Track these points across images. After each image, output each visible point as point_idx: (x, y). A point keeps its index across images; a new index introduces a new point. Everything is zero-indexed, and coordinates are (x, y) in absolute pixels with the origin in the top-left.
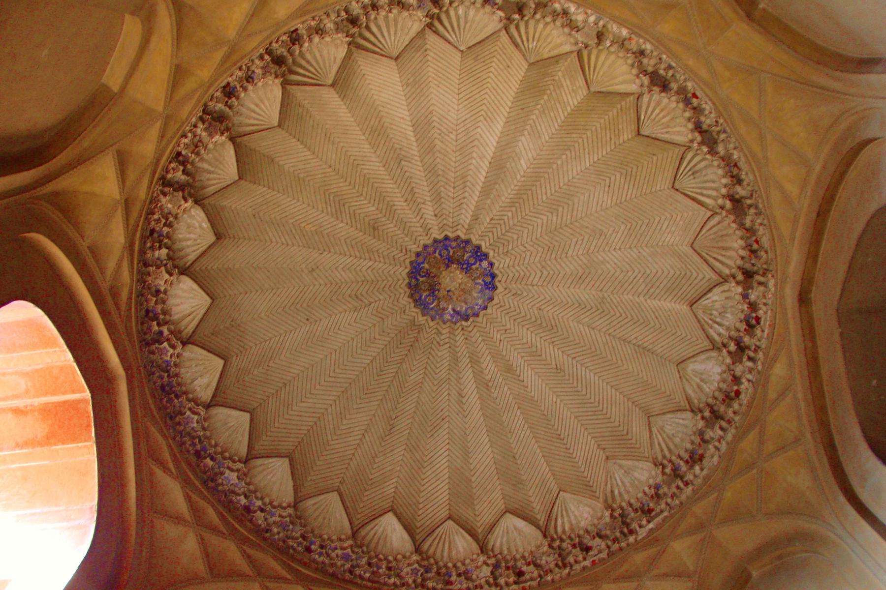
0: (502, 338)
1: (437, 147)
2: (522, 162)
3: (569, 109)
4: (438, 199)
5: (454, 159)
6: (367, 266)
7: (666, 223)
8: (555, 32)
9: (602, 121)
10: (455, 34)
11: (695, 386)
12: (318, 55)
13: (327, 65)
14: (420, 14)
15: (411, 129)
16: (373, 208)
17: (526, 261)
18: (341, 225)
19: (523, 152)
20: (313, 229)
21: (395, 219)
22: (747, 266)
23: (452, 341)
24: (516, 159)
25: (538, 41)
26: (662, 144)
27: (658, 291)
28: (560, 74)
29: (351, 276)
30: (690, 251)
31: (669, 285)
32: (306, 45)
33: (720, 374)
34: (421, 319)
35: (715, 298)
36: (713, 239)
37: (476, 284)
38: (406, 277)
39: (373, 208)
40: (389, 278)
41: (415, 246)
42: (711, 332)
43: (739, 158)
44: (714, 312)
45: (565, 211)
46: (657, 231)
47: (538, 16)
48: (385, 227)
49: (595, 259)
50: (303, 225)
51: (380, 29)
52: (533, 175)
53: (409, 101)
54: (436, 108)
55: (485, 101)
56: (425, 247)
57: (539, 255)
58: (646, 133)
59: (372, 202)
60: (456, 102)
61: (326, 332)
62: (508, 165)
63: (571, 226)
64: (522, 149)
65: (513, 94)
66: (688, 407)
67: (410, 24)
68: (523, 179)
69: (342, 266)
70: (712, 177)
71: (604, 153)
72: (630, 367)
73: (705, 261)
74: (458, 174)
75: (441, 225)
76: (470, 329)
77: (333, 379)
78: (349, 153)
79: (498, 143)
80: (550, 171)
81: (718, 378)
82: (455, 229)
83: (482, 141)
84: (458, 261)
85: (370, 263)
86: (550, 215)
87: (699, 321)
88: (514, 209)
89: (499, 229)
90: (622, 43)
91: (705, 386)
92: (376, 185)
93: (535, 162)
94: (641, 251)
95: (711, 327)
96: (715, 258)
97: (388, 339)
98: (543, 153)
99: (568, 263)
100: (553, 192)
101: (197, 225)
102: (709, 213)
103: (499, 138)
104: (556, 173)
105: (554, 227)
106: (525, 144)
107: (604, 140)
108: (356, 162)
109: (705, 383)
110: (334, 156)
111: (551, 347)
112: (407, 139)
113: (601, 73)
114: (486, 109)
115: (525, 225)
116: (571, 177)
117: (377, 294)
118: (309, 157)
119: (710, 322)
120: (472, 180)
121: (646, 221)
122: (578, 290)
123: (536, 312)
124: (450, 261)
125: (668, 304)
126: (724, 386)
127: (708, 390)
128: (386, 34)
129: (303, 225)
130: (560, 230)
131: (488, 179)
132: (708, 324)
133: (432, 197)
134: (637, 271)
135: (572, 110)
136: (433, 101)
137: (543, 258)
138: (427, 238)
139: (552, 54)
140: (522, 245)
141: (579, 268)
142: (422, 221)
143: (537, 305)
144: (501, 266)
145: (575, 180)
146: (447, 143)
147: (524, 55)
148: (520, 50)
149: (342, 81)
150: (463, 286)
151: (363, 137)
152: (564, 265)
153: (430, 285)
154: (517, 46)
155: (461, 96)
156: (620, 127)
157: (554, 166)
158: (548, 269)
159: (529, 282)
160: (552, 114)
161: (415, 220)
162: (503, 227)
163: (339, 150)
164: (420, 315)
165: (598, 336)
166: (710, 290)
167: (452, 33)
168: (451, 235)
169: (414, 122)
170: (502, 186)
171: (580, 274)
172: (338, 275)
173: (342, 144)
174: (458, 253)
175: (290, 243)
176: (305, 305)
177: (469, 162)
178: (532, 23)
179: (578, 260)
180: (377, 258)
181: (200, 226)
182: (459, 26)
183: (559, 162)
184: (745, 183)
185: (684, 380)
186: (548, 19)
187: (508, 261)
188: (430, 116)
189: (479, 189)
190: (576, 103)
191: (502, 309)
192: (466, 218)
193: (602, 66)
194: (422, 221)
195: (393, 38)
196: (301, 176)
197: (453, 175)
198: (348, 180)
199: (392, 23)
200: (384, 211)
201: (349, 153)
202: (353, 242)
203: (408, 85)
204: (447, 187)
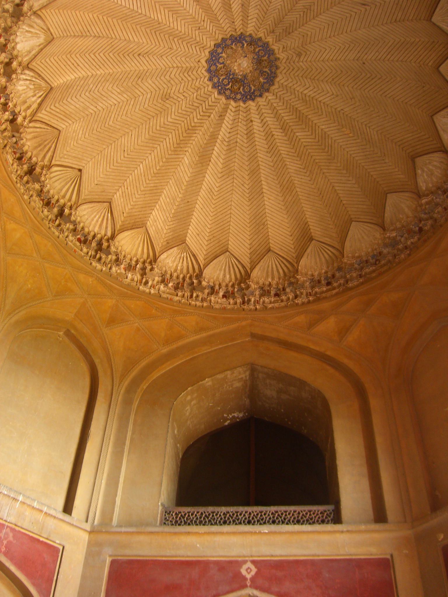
0: (202, 23)
1: (247, 173)
2: (187, 162)
3: (158, 207)
4: (250, 134)
5: (236, 164)
6: (309, 89)
7: (80, 136)
8: (171, 265)
9: (134, 200)
10: (232, 262)
11: (35, 26)
12: (318, 260)
13: (313, 253)
14: (253, 286)
15: (264, 191)
16: (297, 134)
17: (183, 85)
18: (323, 127)
19: (187, 169)
20: (344, 129)
21: (282, 122)
22: (16, 134)
23: (246, 21)
24: (192, 163)
25: (180, 257)
26: (95, 200)
27: (78, 83)
28: (165, 231)
29: (323, 86)
30: (61, 126)
31: (70, 90)
32: (323, 271)
33: (16, 44)
34: (270, 39)
35: (35, 98)
36: (45, 141)
37: (223, 63)
38: (279, 74)
39: (297, 134)
40: (292, 77)
41: (270, 98)
42: (31, 74)
43: (42, 212)
44: (32, 87)
45: (154, 127)
46: (86, 127)
47: (181, 276)
48: (291, 117)
49: (129, 94)
50: (351, 135)
51: (278, 270)
52: (179, 153)
53: (264, 212)
54: (246, 203)
55: (213, 206)
56: (261, 96)
57: (173, 91)
58: (105, 204)
59: (298, 139)
60: (233, 208)
61: (351, 48)
62: (197, 158)
63: (149, 117)
64: (187, 171)
65: (195, 213)
66: (39, 13)
67: (259, 273)
68: (186, 149)
69: (328, 95)
70: (56, 184)
71: (130, 177)
72: (91, 16)
73: (48, 125)
74: (233, 153)
75: (249, 112)
76: (229, 29)
77: (354, 10)
78: (309, 179)
79: (205, 176)
80: (167, 156)
81: (18, 40)
82: (238, 109)
83: (215, 177)
84: (237, 82)
85: (305, 92)
86: (166, 123)
87: (43, 79)
88: (193, 124)
89: (204, 108)
90: (130, 268)
91: (27, 29)
92: (293, 151)
93: (178, 163)
94: (95, 109)
95: (32, 76)
96: (41, 128)
97: (300, 30)
98: (173, 170)
99: (150, 87)
100: (164, 142)
101: (425, 175)
102: (53, 162)
103: (203, 180)
104: (163, 154)
105: (163, 115)
106: (185, 175)
107: (132, 186)
108: (305, 171)
109: (27, 31)
110: (320, 180)
111: (160, 20)
112: (268, 183)
113: (139, 239)
114: (213, 201)
115: (184, 113)
116: (152, 154)
117: (304, 67)
118: (337, 185)
119: (34, 79)
120: (223, 146)
121: (95, 132)
122: (141, 68)
123: (174, 45)
124: (242, 81)
125: (70, 77)
126: (12, 37)
127: (24, 27)
128: (274, 266)
129: (351, 135)
130: (158, 112)
131: (211, 148)
132: (36, 78)
133: (253, 136)
134: (96, 91)
135: (155, 206)
136: (248, 208)
137: (170, 89)
138: (260, 103)
139: (171, 250)
140: (186, 97)
141: (141, 85)
142: (262, 118)
143: (172, 51)
144: (202, 79)
145: (149, 152)
146: (240, 176)
147: (189, 249)
148: (191, 252)
149: (305, 239)
150: (234, 60)
151: (298, 189)
152: (153, 85)
153: (260, 63)
154: (194, 255)
155: (229, 212)
156: (122, 200)
157: (164, 160)
158: (165, 81)
159: (180, 69)
160: (168, 200)
161: (268, 119)
162: (201, 111)
163: (315, 183)
164: (271, 43)
165: (121, 34)
166: (40, 105)
167: (234, 263)
168: (242, 104)
169: (261, 196)
170: (201, 142)
171: (140, 80)
172: (332, 88)
173: (313, 186)
174: (236, 89)
175: (364, 126)
176: (364, 74)
177: (225, 161)
178: (185, 271)
179: (142, 91)
180: (300, 95)
181: (423, 171)
182: (229, 267)
183: (161, 164)
184: (35, 195)
185: (45, 28)
186: (175, 275)
187: (197, 83)
188: (250, 198)
189: (218, 141)
190: (153, 213)
191: (202, 46)
192: (229, 117)
193: (140, 243)
194: (262, 118)
195: (270, 263)
196: (345, 172)
197: (237, 152)
198: (312, 160)
199: (270, 274)
200: (290, 130)
201: (309, 179)
202: (317, 111)
203: (264, 224)
204: (242, 143)
